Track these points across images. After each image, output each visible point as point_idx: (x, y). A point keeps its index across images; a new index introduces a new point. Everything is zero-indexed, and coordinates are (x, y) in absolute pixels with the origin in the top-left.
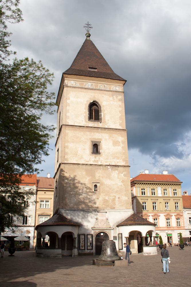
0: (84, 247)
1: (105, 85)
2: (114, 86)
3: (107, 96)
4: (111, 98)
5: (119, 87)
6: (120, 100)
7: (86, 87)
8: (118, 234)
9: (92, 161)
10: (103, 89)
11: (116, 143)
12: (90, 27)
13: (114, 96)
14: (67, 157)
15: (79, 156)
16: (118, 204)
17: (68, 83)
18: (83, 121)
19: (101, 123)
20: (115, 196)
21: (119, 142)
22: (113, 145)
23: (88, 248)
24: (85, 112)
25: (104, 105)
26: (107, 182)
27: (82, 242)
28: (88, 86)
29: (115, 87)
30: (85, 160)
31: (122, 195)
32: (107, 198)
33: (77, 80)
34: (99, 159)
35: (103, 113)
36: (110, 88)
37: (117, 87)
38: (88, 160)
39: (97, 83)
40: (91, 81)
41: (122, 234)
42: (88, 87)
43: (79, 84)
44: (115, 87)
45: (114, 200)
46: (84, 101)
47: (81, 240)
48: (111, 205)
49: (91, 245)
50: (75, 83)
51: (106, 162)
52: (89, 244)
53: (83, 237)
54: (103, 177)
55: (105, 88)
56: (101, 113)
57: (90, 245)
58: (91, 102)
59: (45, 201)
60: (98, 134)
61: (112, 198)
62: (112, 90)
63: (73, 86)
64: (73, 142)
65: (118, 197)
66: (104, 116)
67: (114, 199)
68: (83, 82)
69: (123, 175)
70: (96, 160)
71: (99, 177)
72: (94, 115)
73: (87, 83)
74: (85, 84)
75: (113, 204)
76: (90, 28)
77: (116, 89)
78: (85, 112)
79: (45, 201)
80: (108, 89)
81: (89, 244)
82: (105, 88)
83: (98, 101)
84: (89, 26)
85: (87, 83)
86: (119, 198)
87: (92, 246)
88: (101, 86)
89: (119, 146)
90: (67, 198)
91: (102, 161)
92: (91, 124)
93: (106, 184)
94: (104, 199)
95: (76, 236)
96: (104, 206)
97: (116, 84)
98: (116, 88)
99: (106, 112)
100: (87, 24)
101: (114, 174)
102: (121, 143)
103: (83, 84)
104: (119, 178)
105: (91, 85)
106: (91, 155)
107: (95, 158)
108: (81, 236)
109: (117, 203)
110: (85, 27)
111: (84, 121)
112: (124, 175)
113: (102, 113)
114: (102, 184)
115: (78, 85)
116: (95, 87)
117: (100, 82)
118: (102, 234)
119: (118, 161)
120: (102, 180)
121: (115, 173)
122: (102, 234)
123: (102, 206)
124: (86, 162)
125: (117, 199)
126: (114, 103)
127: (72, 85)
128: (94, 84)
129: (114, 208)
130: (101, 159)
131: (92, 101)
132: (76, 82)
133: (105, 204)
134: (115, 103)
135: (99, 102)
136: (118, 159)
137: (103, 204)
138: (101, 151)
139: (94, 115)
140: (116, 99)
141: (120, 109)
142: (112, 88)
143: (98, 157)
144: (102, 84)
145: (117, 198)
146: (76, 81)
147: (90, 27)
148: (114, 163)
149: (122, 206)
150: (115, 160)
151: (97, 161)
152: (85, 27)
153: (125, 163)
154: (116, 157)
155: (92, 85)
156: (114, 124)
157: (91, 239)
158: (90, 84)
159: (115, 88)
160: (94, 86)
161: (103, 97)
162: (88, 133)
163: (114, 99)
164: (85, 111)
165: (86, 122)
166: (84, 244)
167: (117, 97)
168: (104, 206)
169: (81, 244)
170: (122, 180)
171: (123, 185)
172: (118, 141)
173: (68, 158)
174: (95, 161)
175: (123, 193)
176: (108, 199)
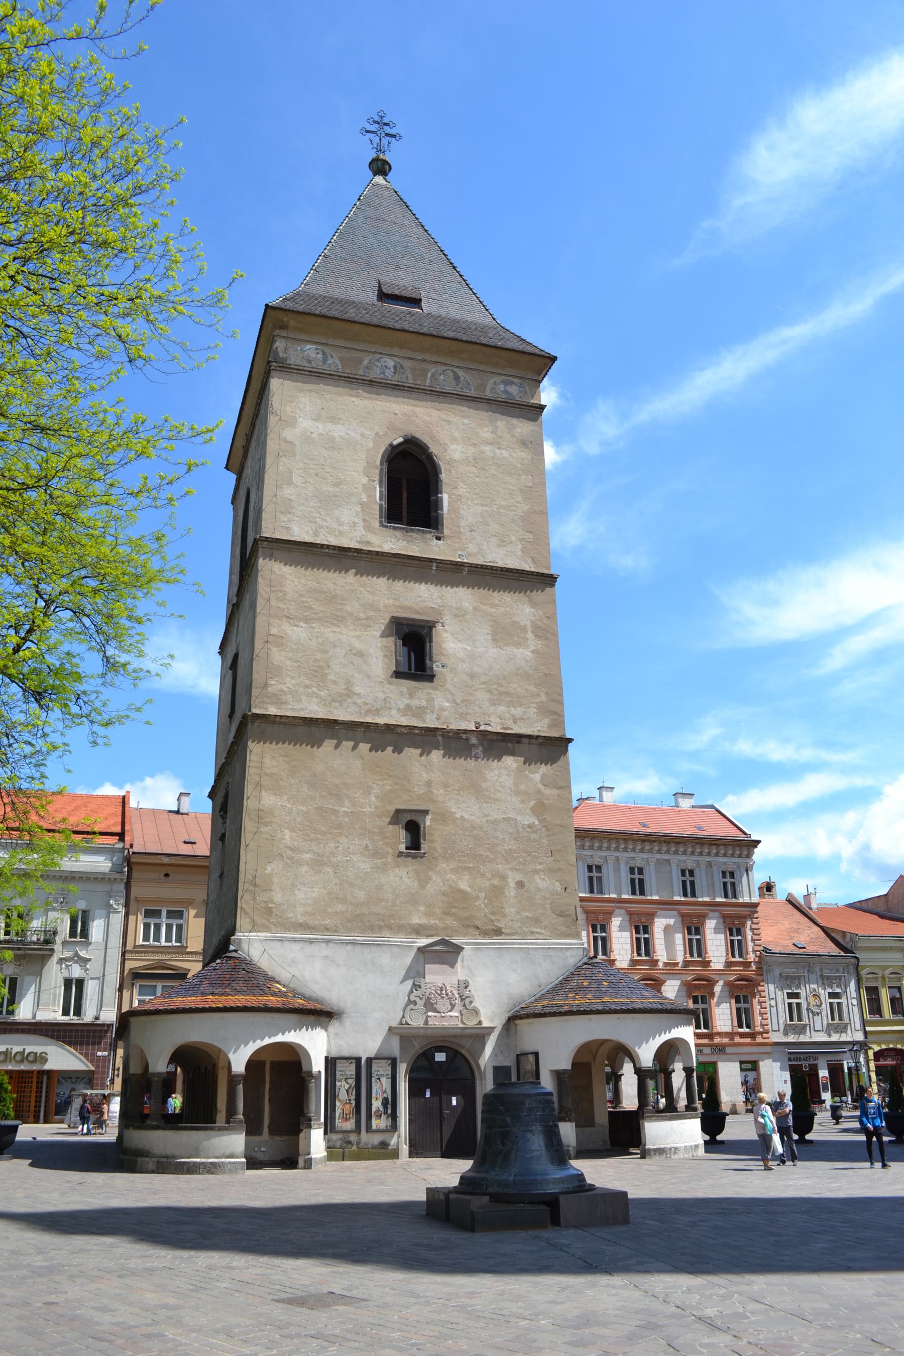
0: (353, 1121)
1: (460, 373)
2: (498, 379)
5: (521, 386)
7: (372, 376)
8: (518, 1056)
9: (394, 712)
10: (448, 389)
11: (504, 633)
12: (387, 135)
14: (280, 686)
15: (334, 682)
16: (518, 913)
17: (291, 351)
18: (355, 524)
19: (438, 538)
20: (503, 878)
21: (524, 629)
22: (495, 640)
23: (374, 1127)
24: (366, 487)
26: (465, 809)
27: (342, 1095)
28: (383, 373)
29: (503, 382)
30: (366, 704)
31: (536, 872)
32: (464, 885)
33: (330, 341)
34: (430, 700)
36: (482, 387)
37: (512, 383)
38: (377, 705)
39: (425, 361)
40: (396, 351)
41: (536, 1055)
42: (382, 376)
43: (341, 360)
44: (505, 383)
45: (497, 892)
46: (362, 435)
47: (338, 1084)
48: (486, 915)
49: (389, 1111)
50: (320, 356)
51: (463, 717)
52: (377, 1104)
53: (351, 1069)
54: (446, 786)
55: (457, 384)
56: (441, 493)
57: (381, 1109)
58: (395, 443)
59: (164, 914)
61: (488, 883)
62: (488, 394)
63: (314, 364)
64: (307, 620)
65: (518, 879)
66: (453, 510)
67: (495, 887)
68: (360, 354)
69: (537, 777)
70: (415, 702)
71: (429, 783)
72: (404, 502)
73: (379, 356)
74: (366, 362)
75: (493, 914)
76: (387, 138)
77: (506, 392)
79: (164, 914)
80: (473, 393)
81: (377, 1104)
82: (457, 384)
83: (425, 439)
84: (386, 128)
85: (378, 361)
86: (520, 884)
87: (394, 1116)
88: (442, 377)
89: (518, 645)
90: (275, 879)
91: (442, 709)
92: (393, 541)
93: (462, 817)
94: (450, 887)
95: (318, 1066)
96: (450, 921)
97: (509, 371)
98: (508, 388)
99: (462, 490)
100: (377, 119)
101: (496, 772)
102: (530, 635)
103: (360, 361)
104: (517, 793)
105: (395, 367)
106: (390, 683)
107: (411, 695)
108: (340, 1066)
109: (510, 910)
110: (368, 132)
111: (362, 524)
113: (445, 497)
114: (445, 817)
115: (334, 363)
116: (414, 379)
117: (435, 358)
118: (440, 1057)
119: (518, 711)
120: (441, 799)
122: (440, 1057)
123: (441, 919)
124: (369, 711)
125: (511, 892)
126: (498, 451)
127: (309, 361)
128: (408, 364)
129: (498, 932)
130: (436, 703)
131: (401, 440)
132: (328, 350)
133: (454, 910)
135: (430, 446)
137: (447, 914)
138: (437, 668)
139: (404, 502)
140: (507, 436)
143: (422, 692)
144: (445, 368)
145: (512, 885)
146: (327, 344)
147: (387, 135)
148: (498, 720)
149: (537, 921)
150: (502, 708)
151: (420, 712)
152: (368, 132)
153: (551, 726)
154: (507, 694)
155: (402, 367)
157: (386, 1083)
158: (391, 363)
159: (502, 387)
160: (410, 375)
164: (365, 480)
165: (368, 528)
166: (353, 1102)
168: (450, 921)
169: (338, 1103)
170: (533, 803)
171: (537, 823)
172: (515, 624)
173: (282, 690)
174: (408, 709)
175: (540, 864)
176: (468, 889)
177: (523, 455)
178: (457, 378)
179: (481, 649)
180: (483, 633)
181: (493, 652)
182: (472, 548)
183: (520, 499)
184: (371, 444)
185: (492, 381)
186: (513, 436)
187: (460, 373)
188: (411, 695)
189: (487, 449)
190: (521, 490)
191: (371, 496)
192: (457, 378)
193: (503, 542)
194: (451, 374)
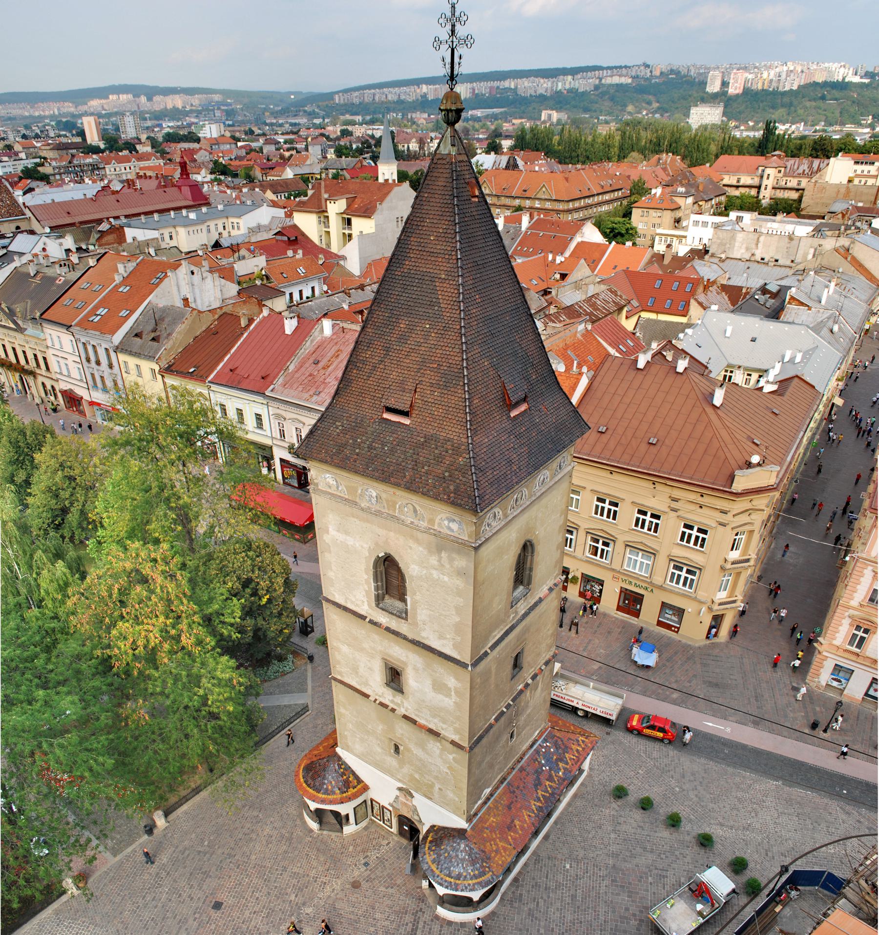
2: (444, 516)
3: (421, 549)
4: (433, 560)
5: (460, 524)
6: (461, 573)
11: (439, 687)
13: (443, 554)
25: (415, 574)
29: (447, 518)
35: (412, 599)
36: (432, 521)
60: (397, 648)
77: (449, 528)
78: (367, 581)
89: (446, 696)
99: (418, 597)
111: (366, 603)
112: (454, 759)
119: (444, 726)
121: (434, 746)
126: (441, 576)
134: (446, 579)
136: (444, 723)
140: (448, 566)
141: (460, 601)
142: (437, 521)
151: (398, 705)
156: (439, 638)
159: (446, 522)
161: (411, 548)
162: (376, 637)
163: (443, 566)
164: (366, 577)
165: (369, 605)
167: (451, 560)
177: (458, 582)
178: (415, 511)
179: (427, 690)
180: (428, 682)
181: (433, 694)
182: (424, 634)
183: (454, 613)
184: (367, 554)
185: (439, 517)
186: (452, 567)
187: (418, 508)
188: (394, 696)
189: (435, 574)
190: (456, 608)
191: (370, 588)
192: (415, 511)
193: (441, 637)
194: (411, 507)
